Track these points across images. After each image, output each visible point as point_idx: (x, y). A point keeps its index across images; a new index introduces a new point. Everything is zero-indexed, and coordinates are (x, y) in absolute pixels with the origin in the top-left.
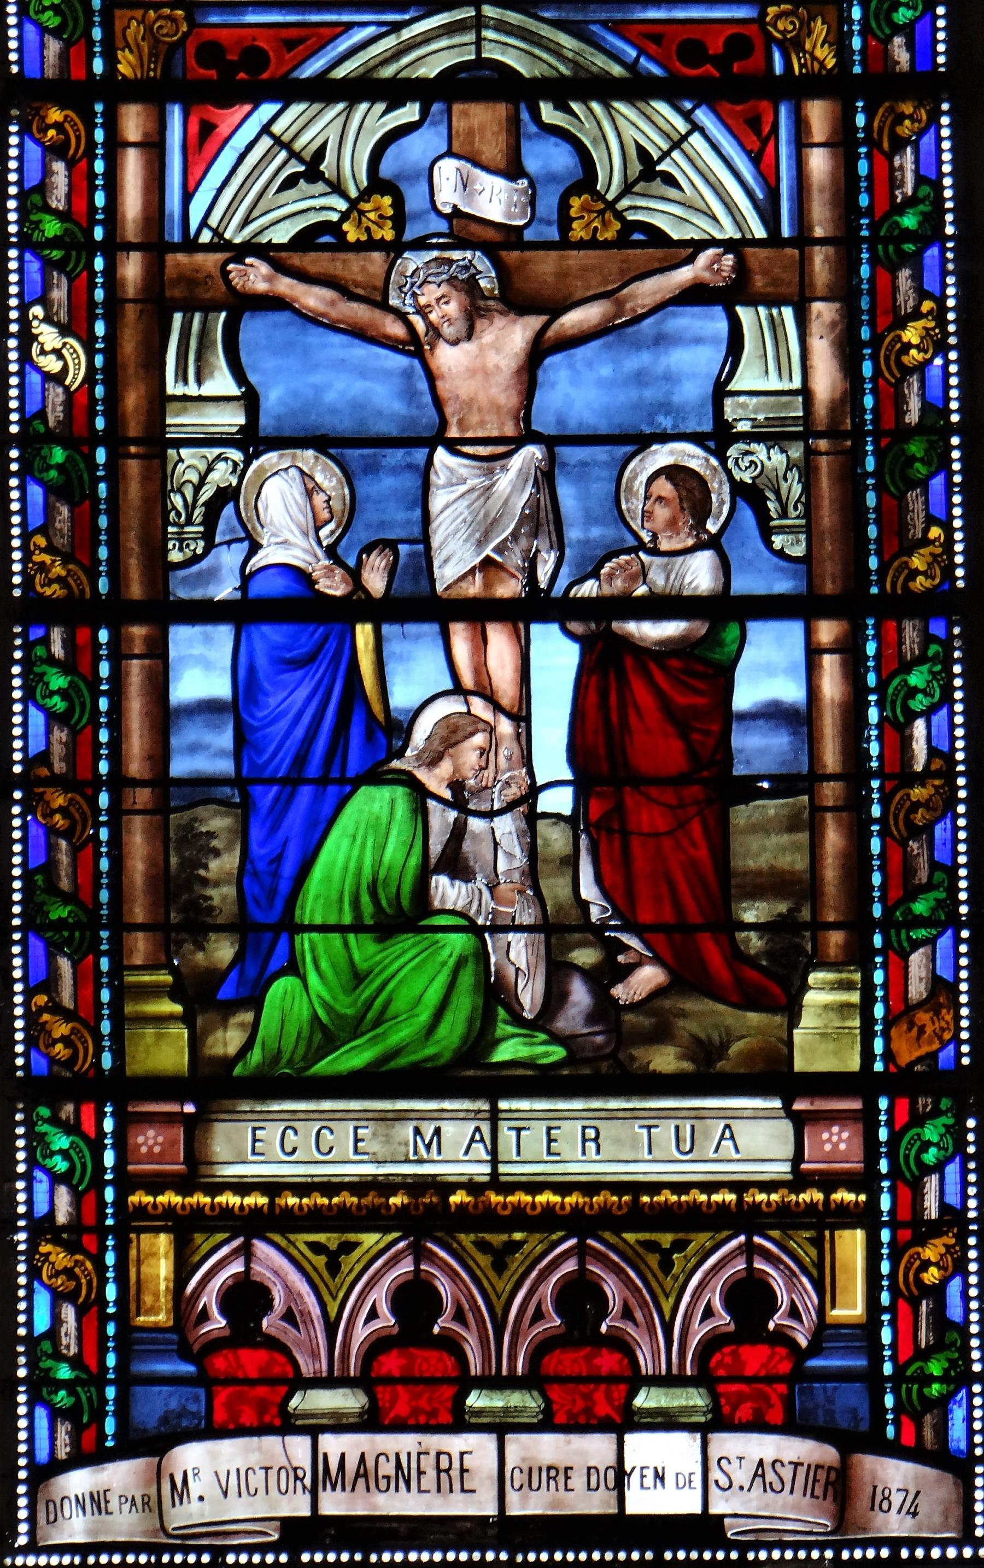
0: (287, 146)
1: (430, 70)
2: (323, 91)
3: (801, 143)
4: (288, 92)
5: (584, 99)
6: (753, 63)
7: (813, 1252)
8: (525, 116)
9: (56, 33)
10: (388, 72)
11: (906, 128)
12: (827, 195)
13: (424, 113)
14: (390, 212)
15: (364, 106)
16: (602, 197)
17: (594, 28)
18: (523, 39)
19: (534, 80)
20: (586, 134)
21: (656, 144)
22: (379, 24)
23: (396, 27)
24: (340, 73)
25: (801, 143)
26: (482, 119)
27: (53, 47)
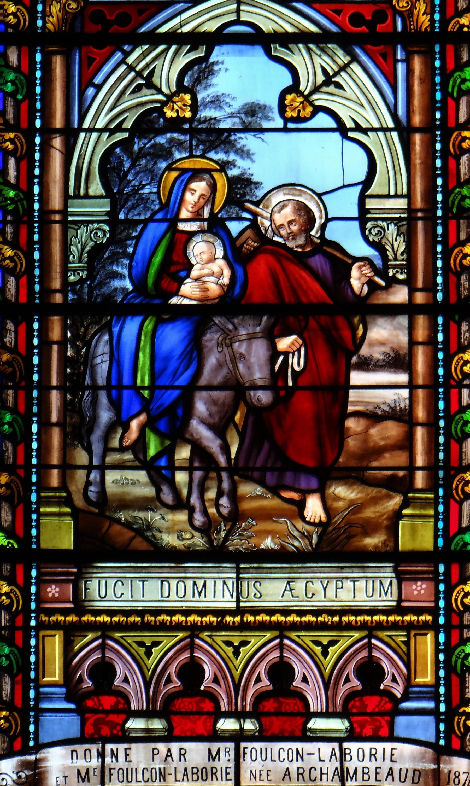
7: (404, 648)
14: (190, 102)
21: (331, 68)
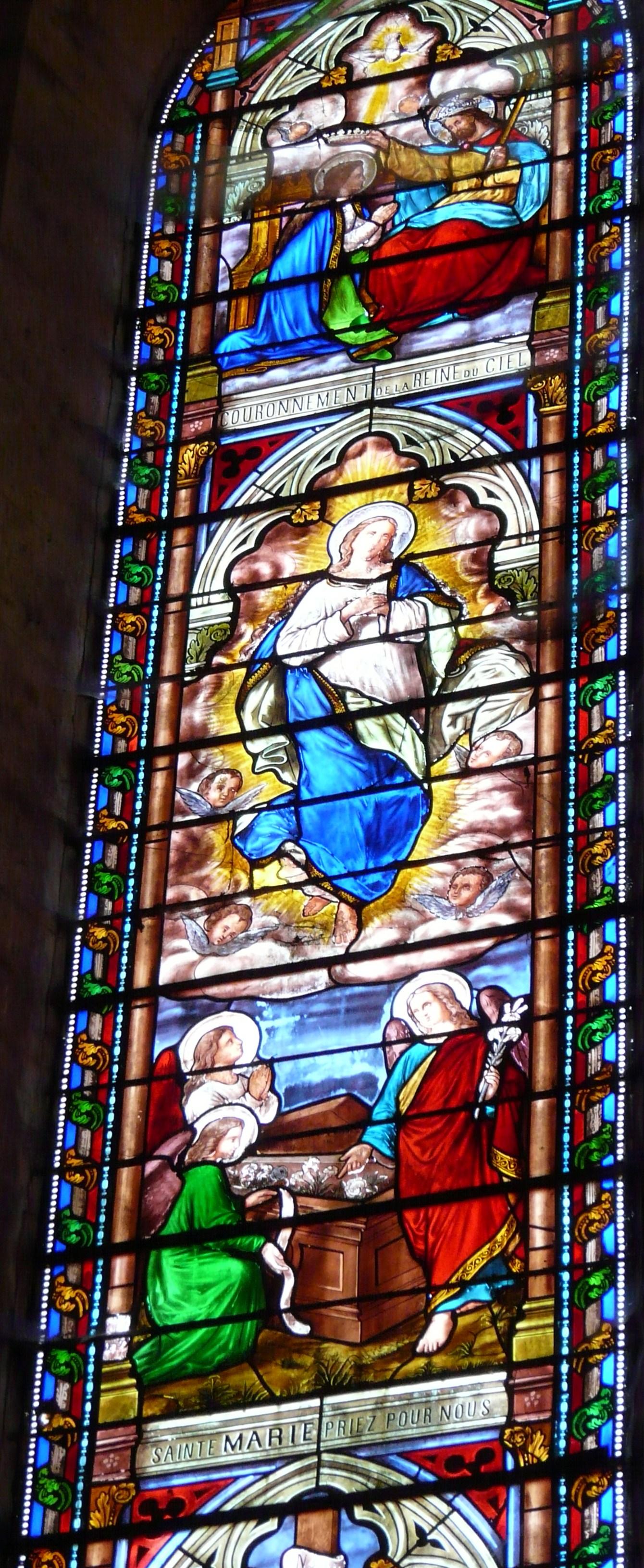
0: (192, 1556)
1: (286, 1498)
2: (218, 1519)
3: (523, 1509)
4: (193, 1523)
5: (382, 1501)
6: (493, 1466)
8: (344, 1516)
9: (53, 1508)
10: (258, 1503)
11: (593, 1492)
12: (540, 1540)
13: (280, 1525)
15: (241, 1526)
16: (391, 1561)
17: (392, 1458)
18: (347, 1470)
19: (352, 1495)
20: (383, 1522)
21: (427, 1523)
22: (255, 1474)
23: (266, 1475)
24: (228, 1507)
25: (523, 1509)
26: (317, 1523)
27: (51, 1515)
